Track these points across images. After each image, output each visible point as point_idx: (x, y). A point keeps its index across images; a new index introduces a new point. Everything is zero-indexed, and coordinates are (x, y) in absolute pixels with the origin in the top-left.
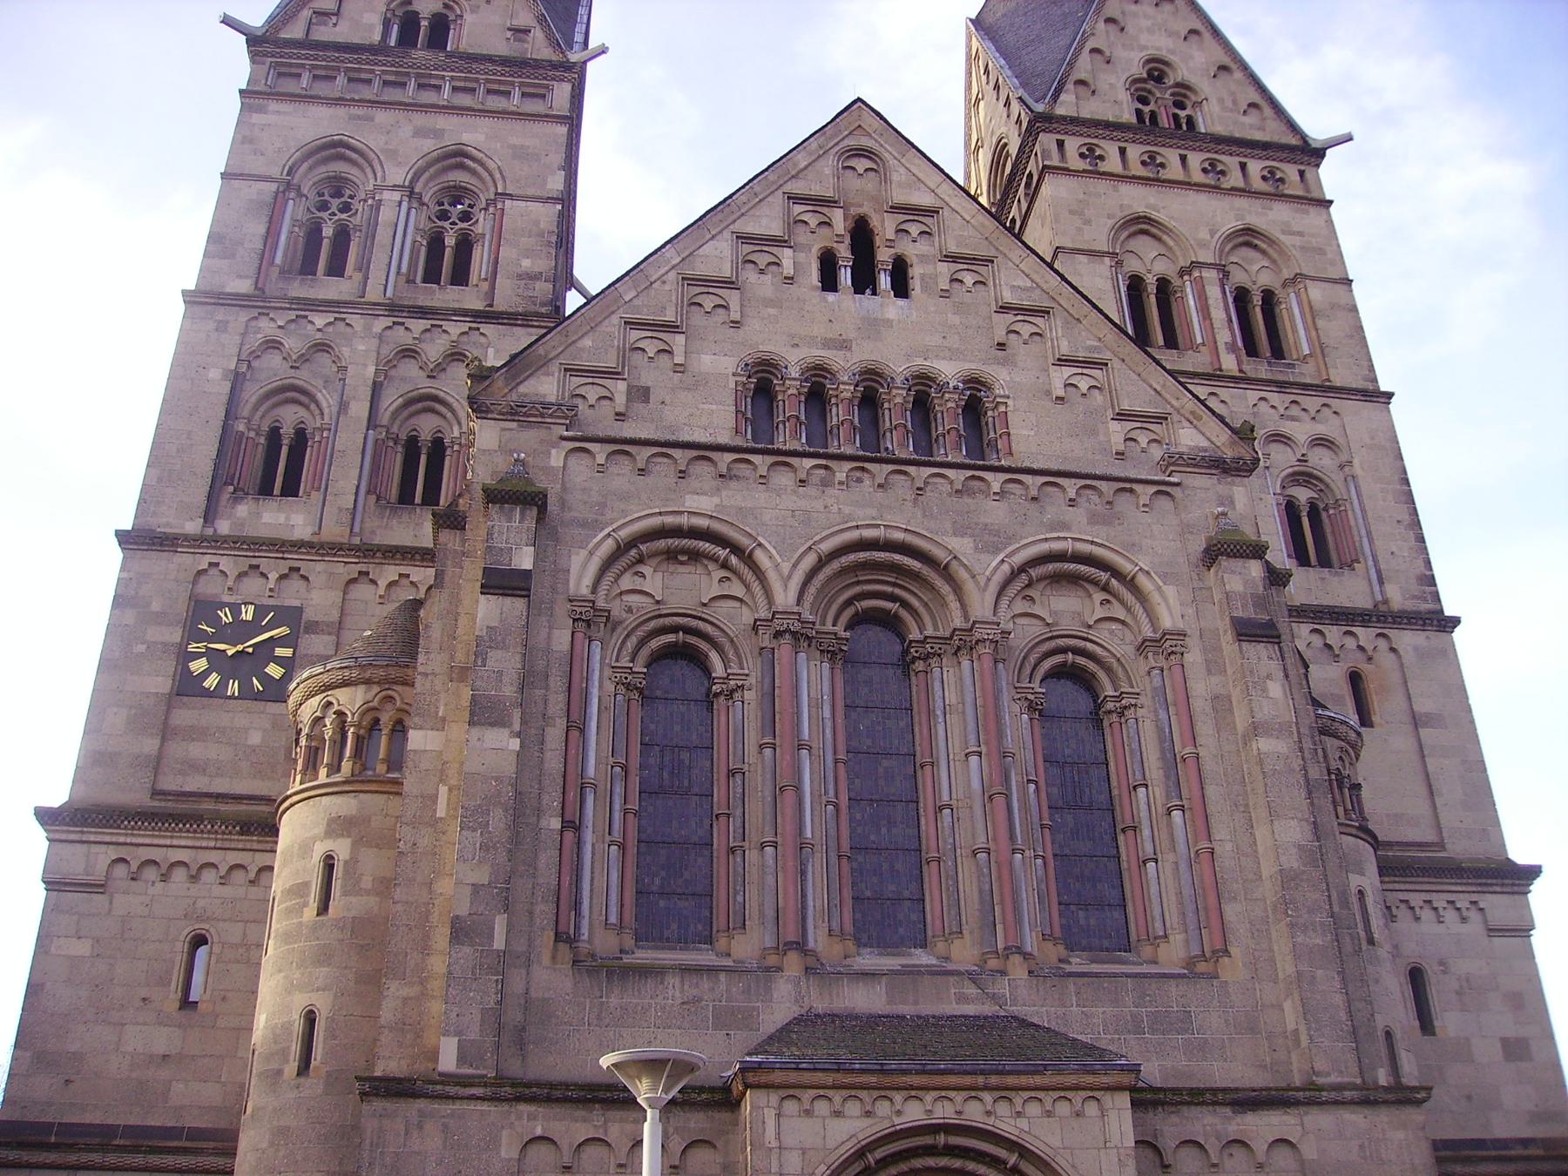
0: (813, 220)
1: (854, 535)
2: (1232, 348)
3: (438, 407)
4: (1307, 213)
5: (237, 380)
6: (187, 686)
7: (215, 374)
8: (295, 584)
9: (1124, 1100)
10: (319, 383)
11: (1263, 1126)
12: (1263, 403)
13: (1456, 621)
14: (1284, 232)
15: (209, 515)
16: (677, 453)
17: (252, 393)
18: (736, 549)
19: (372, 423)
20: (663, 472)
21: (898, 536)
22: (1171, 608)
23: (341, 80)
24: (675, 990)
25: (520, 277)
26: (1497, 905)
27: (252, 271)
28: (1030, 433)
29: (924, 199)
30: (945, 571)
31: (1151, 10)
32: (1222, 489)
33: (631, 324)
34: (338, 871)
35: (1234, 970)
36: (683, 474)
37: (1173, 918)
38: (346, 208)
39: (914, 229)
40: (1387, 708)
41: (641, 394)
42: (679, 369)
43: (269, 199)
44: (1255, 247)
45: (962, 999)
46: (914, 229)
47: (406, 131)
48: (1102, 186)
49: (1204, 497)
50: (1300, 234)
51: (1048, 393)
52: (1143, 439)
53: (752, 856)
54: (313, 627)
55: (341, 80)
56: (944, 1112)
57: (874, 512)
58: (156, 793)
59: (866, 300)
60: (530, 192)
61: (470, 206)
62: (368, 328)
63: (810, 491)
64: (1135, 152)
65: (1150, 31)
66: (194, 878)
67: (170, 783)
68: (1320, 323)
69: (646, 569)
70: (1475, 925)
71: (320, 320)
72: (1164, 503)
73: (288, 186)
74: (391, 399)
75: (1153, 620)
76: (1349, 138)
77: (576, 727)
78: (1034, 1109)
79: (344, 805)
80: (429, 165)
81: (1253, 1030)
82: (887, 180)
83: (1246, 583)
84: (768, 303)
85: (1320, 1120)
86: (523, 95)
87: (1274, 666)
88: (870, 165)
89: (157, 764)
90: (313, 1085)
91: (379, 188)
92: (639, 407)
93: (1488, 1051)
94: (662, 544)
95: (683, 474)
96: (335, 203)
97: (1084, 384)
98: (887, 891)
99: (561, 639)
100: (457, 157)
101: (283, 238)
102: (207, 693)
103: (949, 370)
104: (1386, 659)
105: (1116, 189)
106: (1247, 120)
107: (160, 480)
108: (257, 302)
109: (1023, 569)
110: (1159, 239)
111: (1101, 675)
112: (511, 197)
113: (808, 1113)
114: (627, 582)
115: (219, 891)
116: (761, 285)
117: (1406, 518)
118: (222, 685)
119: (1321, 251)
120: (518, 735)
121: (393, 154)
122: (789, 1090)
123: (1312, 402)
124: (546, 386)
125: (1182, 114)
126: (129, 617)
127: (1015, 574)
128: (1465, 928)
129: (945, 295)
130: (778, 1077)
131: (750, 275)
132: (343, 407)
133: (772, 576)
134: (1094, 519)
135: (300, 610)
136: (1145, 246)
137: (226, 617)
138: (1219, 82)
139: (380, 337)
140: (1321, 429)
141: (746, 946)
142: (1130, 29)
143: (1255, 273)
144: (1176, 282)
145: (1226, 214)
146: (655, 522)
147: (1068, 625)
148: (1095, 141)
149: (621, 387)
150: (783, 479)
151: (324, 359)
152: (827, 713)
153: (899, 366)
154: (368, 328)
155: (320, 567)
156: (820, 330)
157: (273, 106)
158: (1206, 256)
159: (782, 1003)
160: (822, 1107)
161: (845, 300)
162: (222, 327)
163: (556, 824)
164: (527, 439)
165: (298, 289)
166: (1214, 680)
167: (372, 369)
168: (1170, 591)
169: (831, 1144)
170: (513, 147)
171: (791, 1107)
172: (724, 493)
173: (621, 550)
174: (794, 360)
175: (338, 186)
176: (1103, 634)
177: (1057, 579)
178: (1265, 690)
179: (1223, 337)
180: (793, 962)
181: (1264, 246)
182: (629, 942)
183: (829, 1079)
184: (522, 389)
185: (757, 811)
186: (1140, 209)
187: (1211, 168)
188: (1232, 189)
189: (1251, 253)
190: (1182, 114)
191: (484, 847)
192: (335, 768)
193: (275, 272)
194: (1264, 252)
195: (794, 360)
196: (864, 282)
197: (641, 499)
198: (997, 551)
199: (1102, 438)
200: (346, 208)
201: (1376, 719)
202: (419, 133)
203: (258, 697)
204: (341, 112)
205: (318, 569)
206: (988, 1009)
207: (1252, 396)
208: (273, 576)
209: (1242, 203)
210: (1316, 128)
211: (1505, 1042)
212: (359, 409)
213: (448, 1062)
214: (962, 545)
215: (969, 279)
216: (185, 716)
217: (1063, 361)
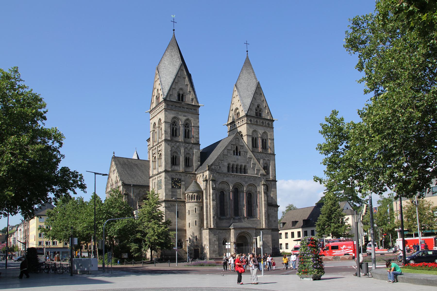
5: (171, 151)
6: (173, 187)
24: (225, 221)
26: (275, 209)
29: (242, 145)
38: (176, 125)
41: (220, 167)
54: (183, 181)
59: (237, 157)
64: (255, 120)
71: (178, 144)
79: (197, 204)
82: (239, 141)
84: (230, 157)
90: (197, 226)
93: (273, 221)
103: (243, 164)
108: (171, 141)
136: (255, 134)
141: (228, 216)
150: (231, 177)
174: (232, 163)
185: (228, 206)
187: (263, 123)
192: (194, 199)
195: (232, 163)
196: (237, 155)
205: (182, 174)
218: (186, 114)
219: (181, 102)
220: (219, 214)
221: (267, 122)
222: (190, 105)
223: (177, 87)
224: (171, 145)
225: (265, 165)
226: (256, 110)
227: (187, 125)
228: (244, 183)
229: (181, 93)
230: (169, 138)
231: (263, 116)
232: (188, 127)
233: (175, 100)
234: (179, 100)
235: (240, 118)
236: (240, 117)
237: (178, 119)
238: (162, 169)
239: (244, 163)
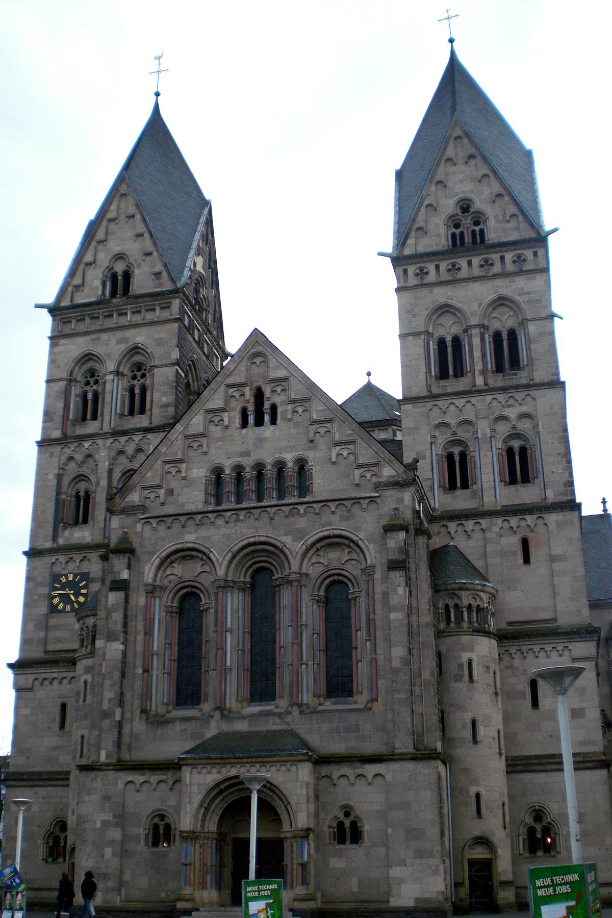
0: (237, 395)
5: (59, 477)
6: (53, 609)
7: (51, 477)
8: (86, 562)
10: (90, 472)
11: (371, 770)
12: (494, 401)
14: (520, 295)
15: (55, 538)
16: (181, 518)
17: (66, 481)
18: (205, 554)
19: (110, 486)
20: (177, 527)
21: (263, 539)
23: (88, 320)
24: (178, 727)
25: (162, 407)
27: (60, 426)
31: (461, 167)
32: (399, 495)
33: (165, 462)
34: (88, 685)
36: (184, 526)
37: (365, 685)
38: (96, 382)
39: (279, 389)
41: (170, 492)
42: (184, 478)
43: (64, 389)
44: (506, 305)
45: (275, 724)
46: (279, 389)
47: (113, 342)
48: (424, 292)
49: (390, 499)
50: (529, 293)
51: (330, 459)
52: (368, 475)
54: (93, 580)
55: (88, 320)
57: (254, 530)
58: (46, 652)
59: (259, 430)
60: (165, 362)
62: (104, 444)
63: (231, 525)
64: (444, 266)
65: (461, 182)
66: (60, 683)
67: (50, 648)
68: (532, 346)
69: (175, 565)
71: (86, 445)
72: (374, 505)
73: (71, 381)
77: (148, 633)
78: (273, 769)
80: (125, 356)
81: (383, 730)
83: (396, 543)
84: (219, 439)
85: (396, 766)
86: (162, 308)
87: (402, 581)
88: (261, 359)
89: (45, 641)
91: (105, 375)
92: (170, 499)
94: (179, 555)
95: (184, 526)
96: (92, 380)
97: (345, 453)
98: (262, 683)
99: (142, 601)
100: (135, 350)
101: (72, 406)
102: (60, 611)
103: (289, 458)
104: (541, 529)
105: (431, 292)
106: (509, 226)
108: (64, 440)
109: (314, 544)
110: (454, 314)
112: (156, 367)
113: (200, 773)
114: (168, 572)
115: (69, 687)
116: (215, 431)
117: (563, 451)
118: (65, 607)
119: (539, 301)
121: (109, 355)
122: (194, 766)
123: (519, 396)
124: (134, 497)
125: (477, 228)
126: (31, 585)
127: (308, 550)
129: (290, 420)
130: (189, 762)
131: (212, 428)
132: (98, 483)
134: (342, 518)
135: (88, 573)
137: (64, 580)
138: (497, 205)
139: (109, 448)
140: (524, 409)
141: (207, 707)
142: (450, 184)
143: (504, 321)
145: (486, 292)
146: (174, 548)
147: (335, 564)
149: (162, 491)
150: (220, 522)
151: (90, 461)
152: (240, 614)
153: (269, 460)
154: (104, 444)
155: (93, 555)
156: (239, 448)
157: (62, 341)
158: (474, 321)
160: (204, 771)
161: (252, 432)
163: (140, 671)
164: (130, 520)
165: (80, 431)
166: (384, 585)
167: (107, 464)
168: (371, 547)
169: (207, 782)
170: (156, 340)
171: (195, 771)
173: (162, 562)
175: (92, 373)
176: (348, 567)
177: (330, 545)
178: (396, 592)
180: (217, 715)
181: (510, 304)
182: (171, 708)
183: (205, 761)
184: (127, 500)
186: (442, 300)
188: (494, 275)
189: (505, 309)
191: (112, 685)
193: (69, 423)
194: (510, 307)
197: (169, 540)
198: (302, 539)
199: (351, 477)
200: (96, 382)
202: (119, 342)
204: (87, 338)
206: (284, 727)
207: (488, 398)
208: (78, 561)
209: (498, 282)
212: (104, 483)
213: (103, 758)
214: (287, 540)
215: (300, 410)
216: (53, 621)
217: (337, 444)
218: (128, 333)
224: (61, 454)
225: (516, 444)
230: (57, 434)
239: (291, 449)
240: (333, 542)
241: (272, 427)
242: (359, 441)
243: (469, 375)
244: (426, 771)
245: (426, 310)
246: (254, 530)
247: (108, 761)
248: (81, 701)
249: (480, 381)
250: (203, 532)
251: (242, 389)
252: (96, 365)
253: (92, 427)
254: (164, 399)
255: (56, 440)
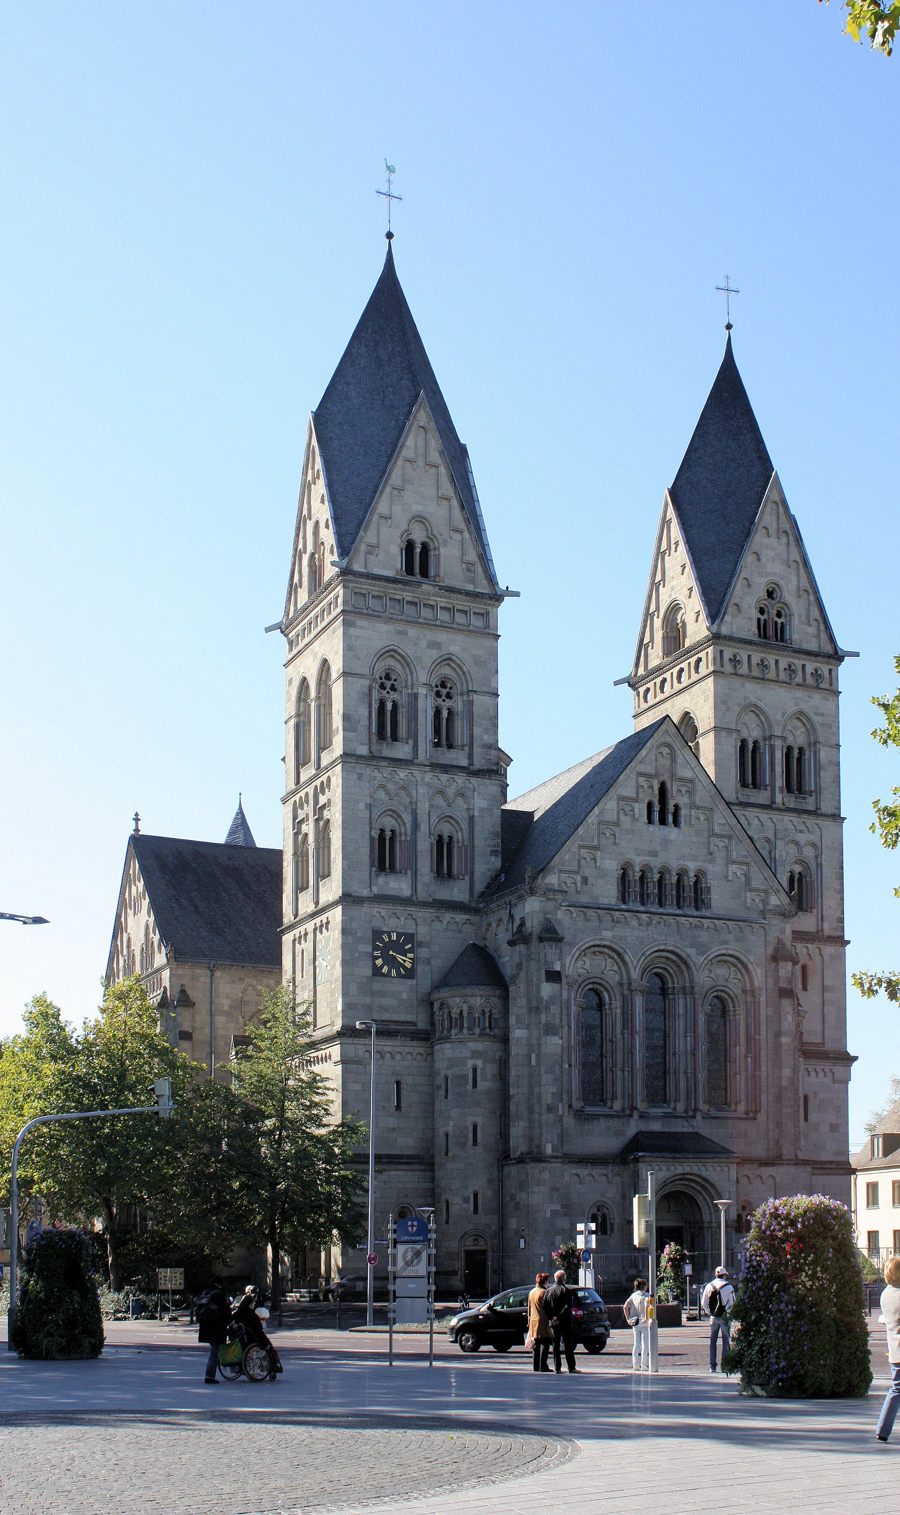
1: (656, 948)
2: (782, 791)
3: (452, 821)
4: (828, 700)
5: (370, 807)
7: (362, 806)
9: (735, 1166)
10: (403, 809)
13: (848, 942)
14: (816, 714)
22: (759, 977)
24: (603, 1123)
26: (839, 1070)
27: (367, 741)
28: (720, 898)
30: (685, 963)
35: (762, 1117)
37: (743, 1096)
38: (393, 688)
40: (814, 982)
45: (683, 1126)
48: (737, 682)
50: (822, 715)
53: (619, 1073)
56: (687, 1169)
60: (484, 689)
61: (450, 688)
62: (423, 779)
68: (822, 773)
69: (585, 959)
70: (828, 1080)
71: (402, 774)
74: (434, 819)
75: (751, 980)
76: (857, 655)
85: (783, 1169)
107: (349, 866)
108: (373, 758)
111: (729, 1000)
120: (562, 1038)
121: (419, 659)
123: (811, 821)
125: (779, 621)
128: (825, 1080)
132: (416, 826)
133: (630, 966)
141: (617, 1106)
143: (798, 738)
144: (762, 743)
148: (737, 651)
154: (423, 779)
159: (633, 1127)
162: (360, 777)
165: (387, 752)
167: (427, 804)
172: (616, 929)
179: (780, 782)
186: (753, 699)
190: (779, 621)
201: (809, 987)
203: (404, 977)
206: (690, 1130)
210: (843, 644)
211: (831, 1125)
219: (418, 578)
220: (576, 1092)
221: (810, 668)
222: (459, 591)
223: (397, 509)
225: (797, 869)
226: (762, 611)
227: (443, 689)
228: (692, 952)
229: (419, 536)
230: (363, 750)
231: (795, 637)
232: (449, 696)
233: (390, 573)
234: (410, 570)
235: (688, 651)
236: (688, 643)
237: (405, 661)
238: (332, 889)
240: (723, 960)
241: (676, 830)
242: (753, 864)
243: (769, 788)
244: (804, 1175)
245: (739, 705)
246: (664, 937)
247: (555, 1154)
248: (470, 1087)
249: (779, 798)
250: (619, 931)
251: (651, 780)
252: (398, 667)
253: (402, 751)
254: (486, 737)
255: (360, 757)
